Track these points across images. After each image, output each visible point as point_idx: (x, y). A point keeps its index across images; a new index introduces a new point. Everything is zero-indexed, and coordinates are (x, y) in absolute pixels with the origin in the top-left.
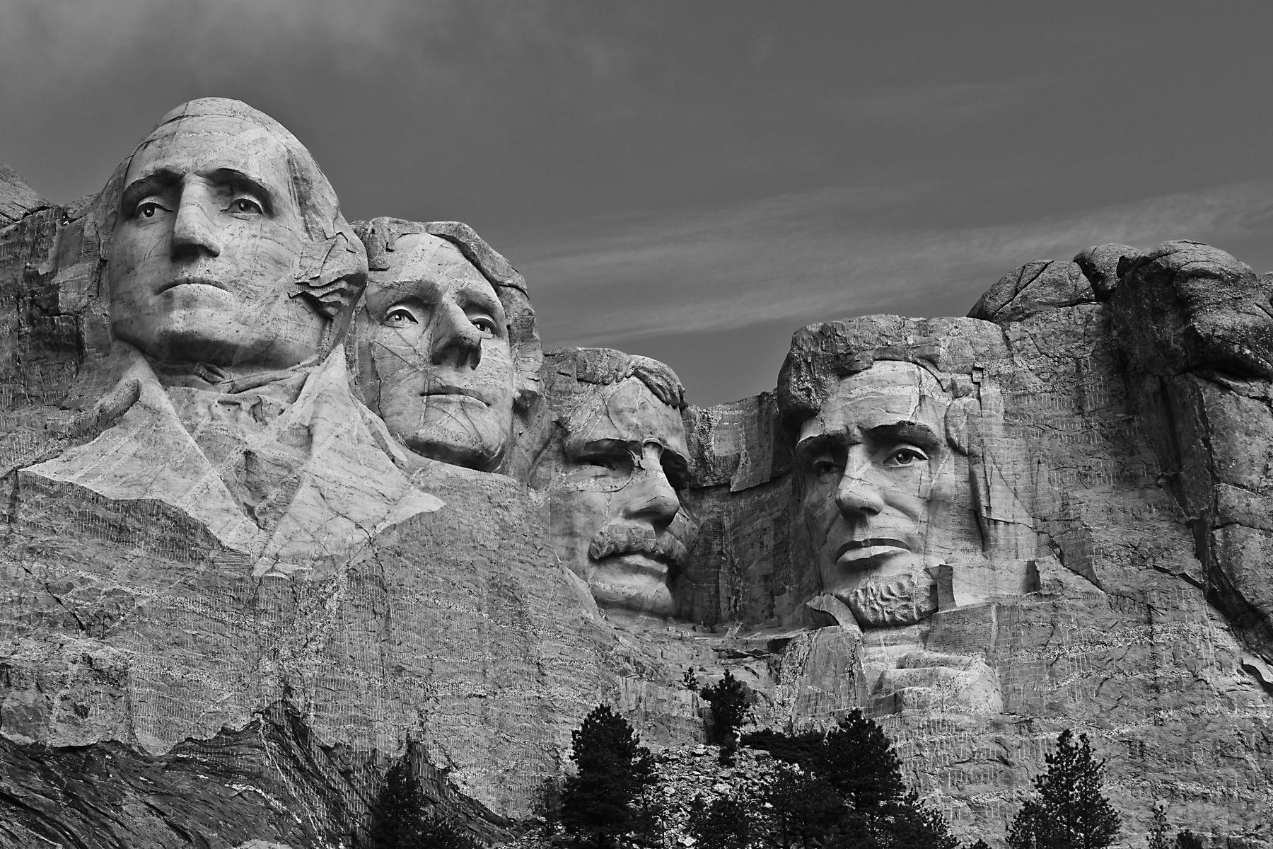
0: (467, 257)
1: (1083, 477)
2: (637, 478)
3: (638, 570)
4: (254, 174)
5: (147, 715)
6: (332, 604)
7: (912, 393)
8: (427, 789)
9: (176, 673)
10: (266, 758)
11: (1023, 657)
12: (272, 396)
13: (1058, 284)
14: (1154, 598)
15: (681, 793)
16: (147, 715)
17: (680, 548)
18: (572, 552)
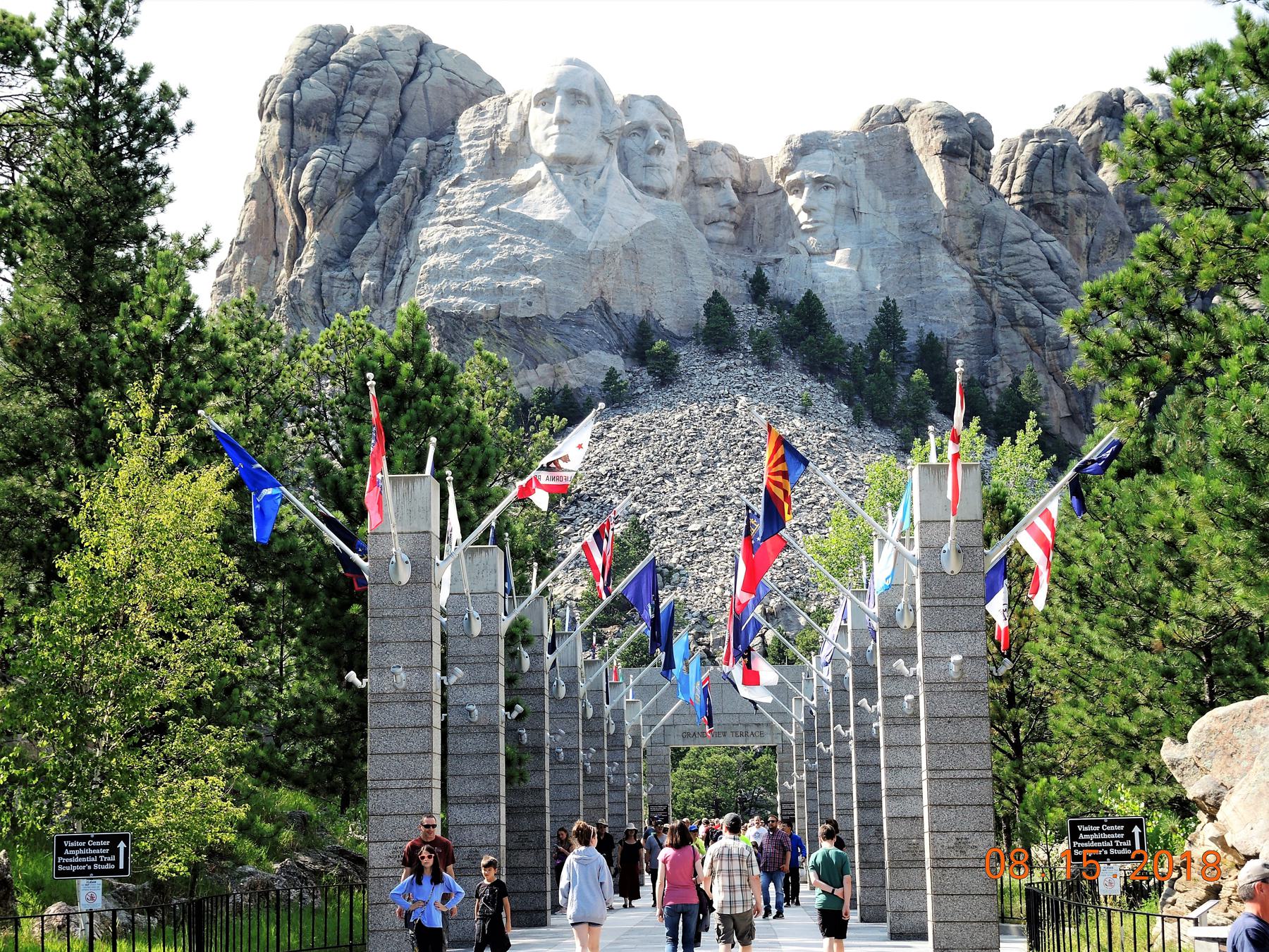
0: (659, 109)
1: (895, 195)
2: (722, 191)
3: (723, 228)
4: (584, 91)
5: (553, 304)
6: (617, 260)
7: (829, 162)
8: (653, 328)
9: (562, 288)
10: (594, 318)
11: (871, 268)
12: (592, 178)
13: (886, 115)
14: (920, 245)
15: (744, 326)
16: (553, 304)
17: (738, 219)
18: (698, 221)
